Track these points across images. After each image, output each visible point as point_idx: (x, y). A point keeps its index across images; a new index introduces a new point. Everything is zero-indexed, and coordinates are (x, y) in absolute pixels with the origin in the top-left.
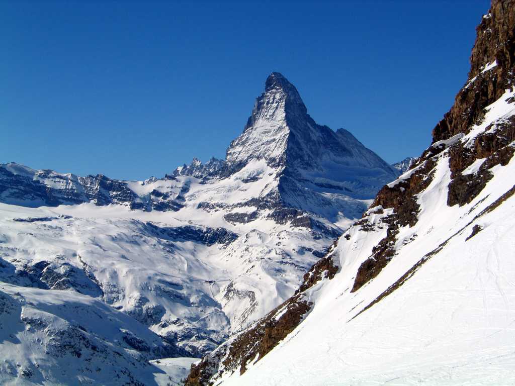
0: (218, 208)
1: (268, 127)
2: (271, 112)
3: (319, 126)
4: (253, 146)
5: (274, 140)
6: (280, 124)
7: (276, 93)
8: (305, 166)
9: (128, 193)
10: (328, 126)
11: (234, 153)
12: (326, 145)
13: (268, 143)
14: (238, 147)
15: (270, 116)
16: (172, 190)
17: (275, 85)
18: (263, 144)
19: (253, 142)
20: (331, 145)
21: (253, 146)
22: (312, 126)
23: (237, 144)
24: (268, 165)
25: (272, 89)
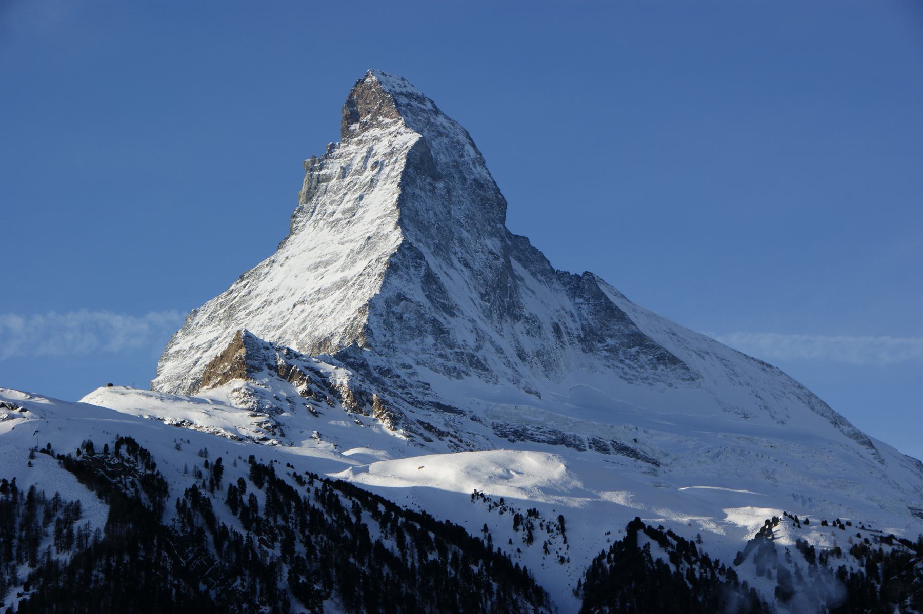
2: (349, 200)
3: (562, 276)
6: (373, 229)
7: (377, 139)
8: (450, 364)
10: (597, 272)
11: (191, 348)
12: (589, 339)
13: (321, 295)
15: (343, 213)
17: (378, 112)
19: (267, 303)
20: (610, 341)
22: (534, 274)
23: (211, 318)
25: (365, 127)
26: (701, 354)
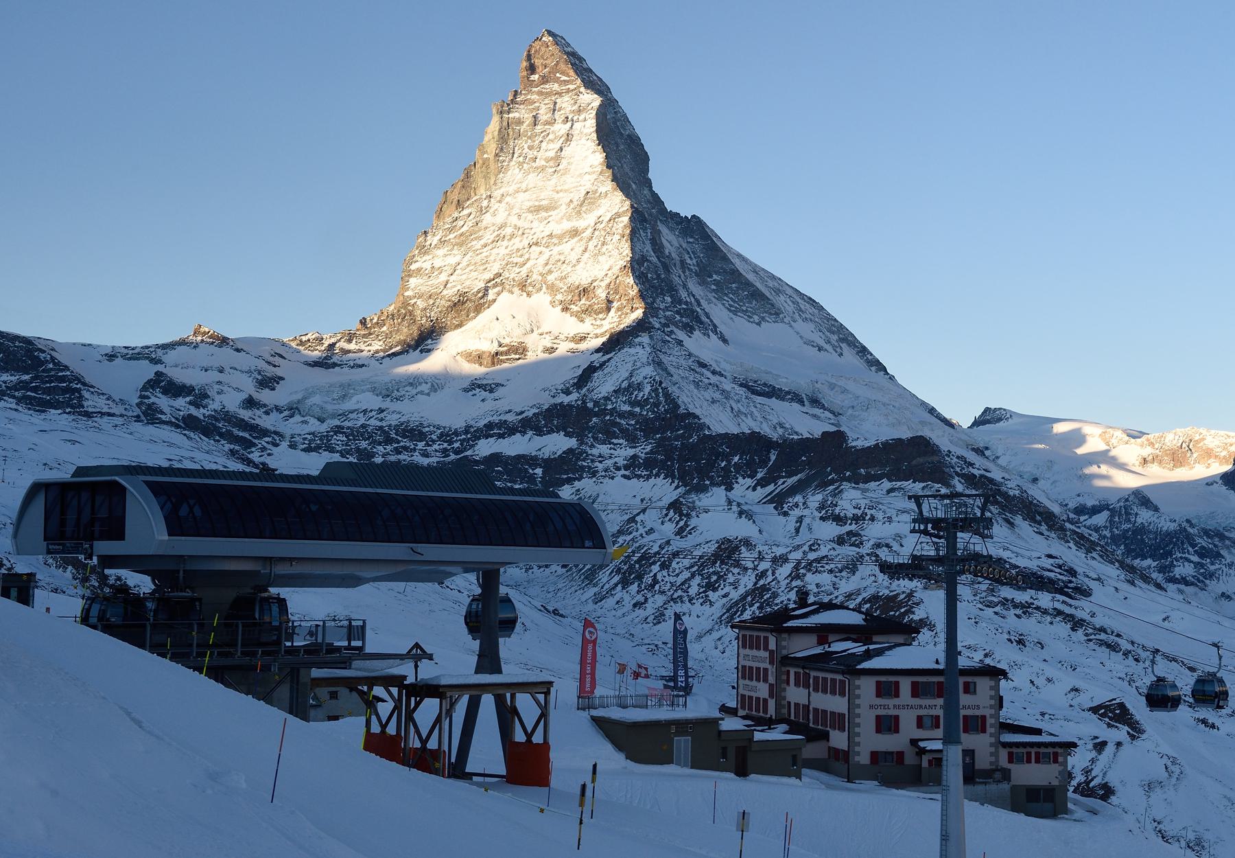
0: (405, 442)
1: (546, 195)
4: (502, 250)
5: (575, 233)
6: (587, 183)
9: (62, 379)
12: (703, 274)
13: (555, 240)
14: (440, 252)
15: (547, 160)
16: (221, 377)
18: (537, 244)
20: (715, 277)
21: (502, 251)
23: (442, 242)
24: (565, 309)
26: (778, 292)
